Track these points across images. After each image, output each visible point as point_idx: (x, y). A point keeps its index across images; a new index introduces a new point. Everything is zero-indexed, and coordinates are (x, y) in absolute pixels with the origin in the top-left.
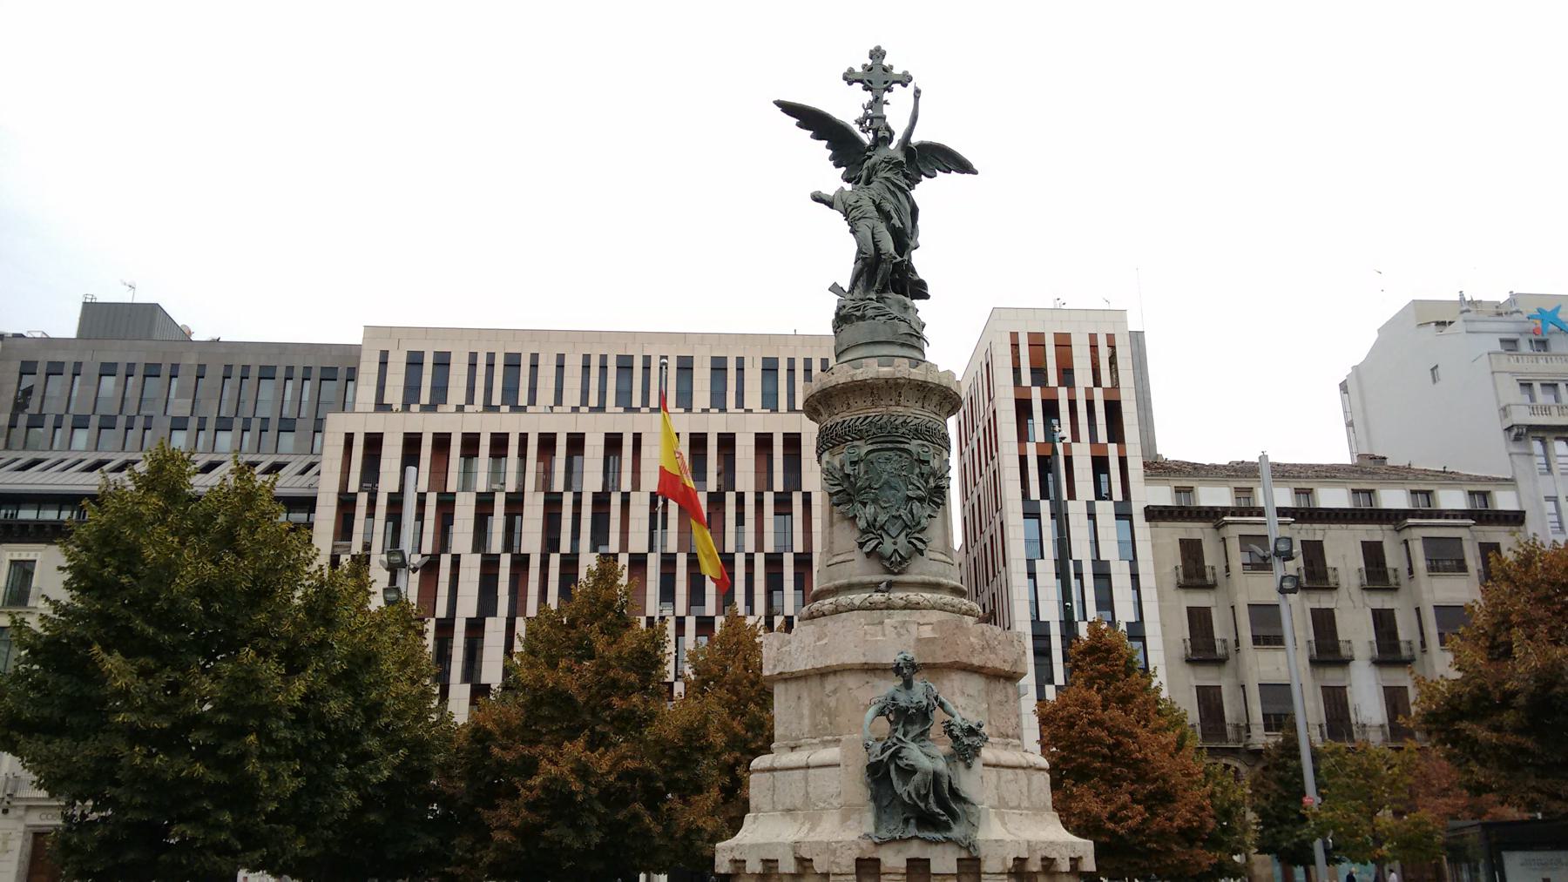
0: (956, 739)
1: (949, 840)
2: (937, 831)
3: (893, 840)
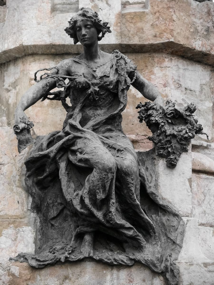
0: (154, 126)
1: (137, 263)
2: (123, 250)
3: (57, 263)
